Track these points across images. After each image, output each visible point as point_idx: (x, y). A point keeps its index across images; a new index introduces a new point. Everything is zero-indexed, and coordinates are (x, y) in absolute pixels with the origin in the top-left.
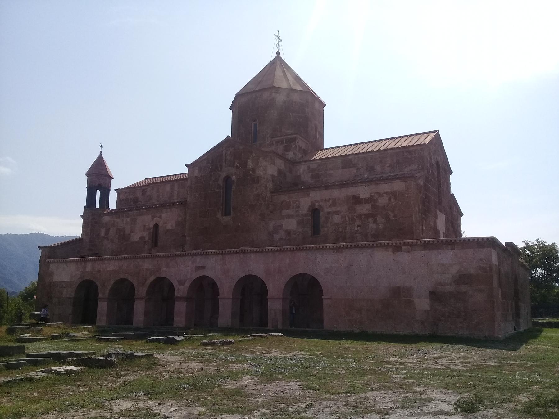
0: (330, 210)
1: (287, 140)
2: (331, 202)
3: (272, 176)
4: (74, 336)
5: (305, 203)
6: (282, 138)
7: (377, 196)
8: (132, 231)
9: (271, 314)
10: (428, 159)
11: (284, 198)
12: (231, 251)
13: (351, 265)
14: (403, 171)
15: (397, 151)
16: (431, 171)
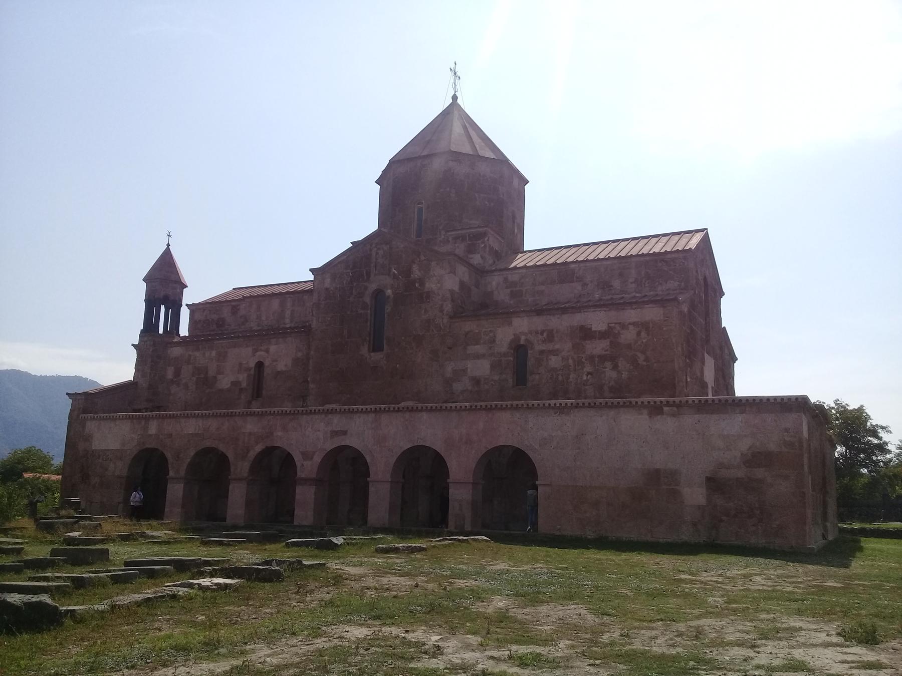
0: (544, 348)
2: (545, 335)
3: (452, 292)
4: (153, 537)
5: (504, 336)
6: (464, 232)
8: (220, 372)
9: (453, 508)
11: (469, 326)
12: (389, 408)
13: (583, 434)
14: (656, 291)
15: (648, 258)
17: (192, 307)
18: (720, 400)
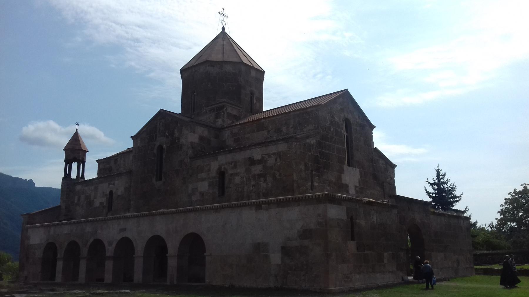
0: (232, 172)
1: (217, 108)
2: (233, 164)
3: (192, 143)
6: (213, 106)
7: (267, 157)
10: (327, 118)
13: (225, 224)
15: (298, 112)
16: (332, 129)
17: (100, 162)
18: (286, 199)
